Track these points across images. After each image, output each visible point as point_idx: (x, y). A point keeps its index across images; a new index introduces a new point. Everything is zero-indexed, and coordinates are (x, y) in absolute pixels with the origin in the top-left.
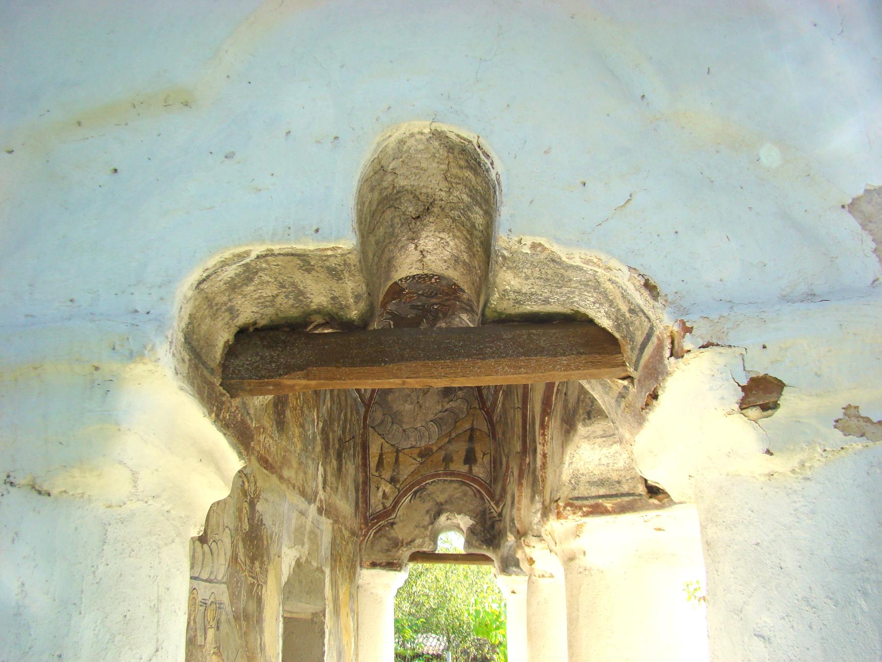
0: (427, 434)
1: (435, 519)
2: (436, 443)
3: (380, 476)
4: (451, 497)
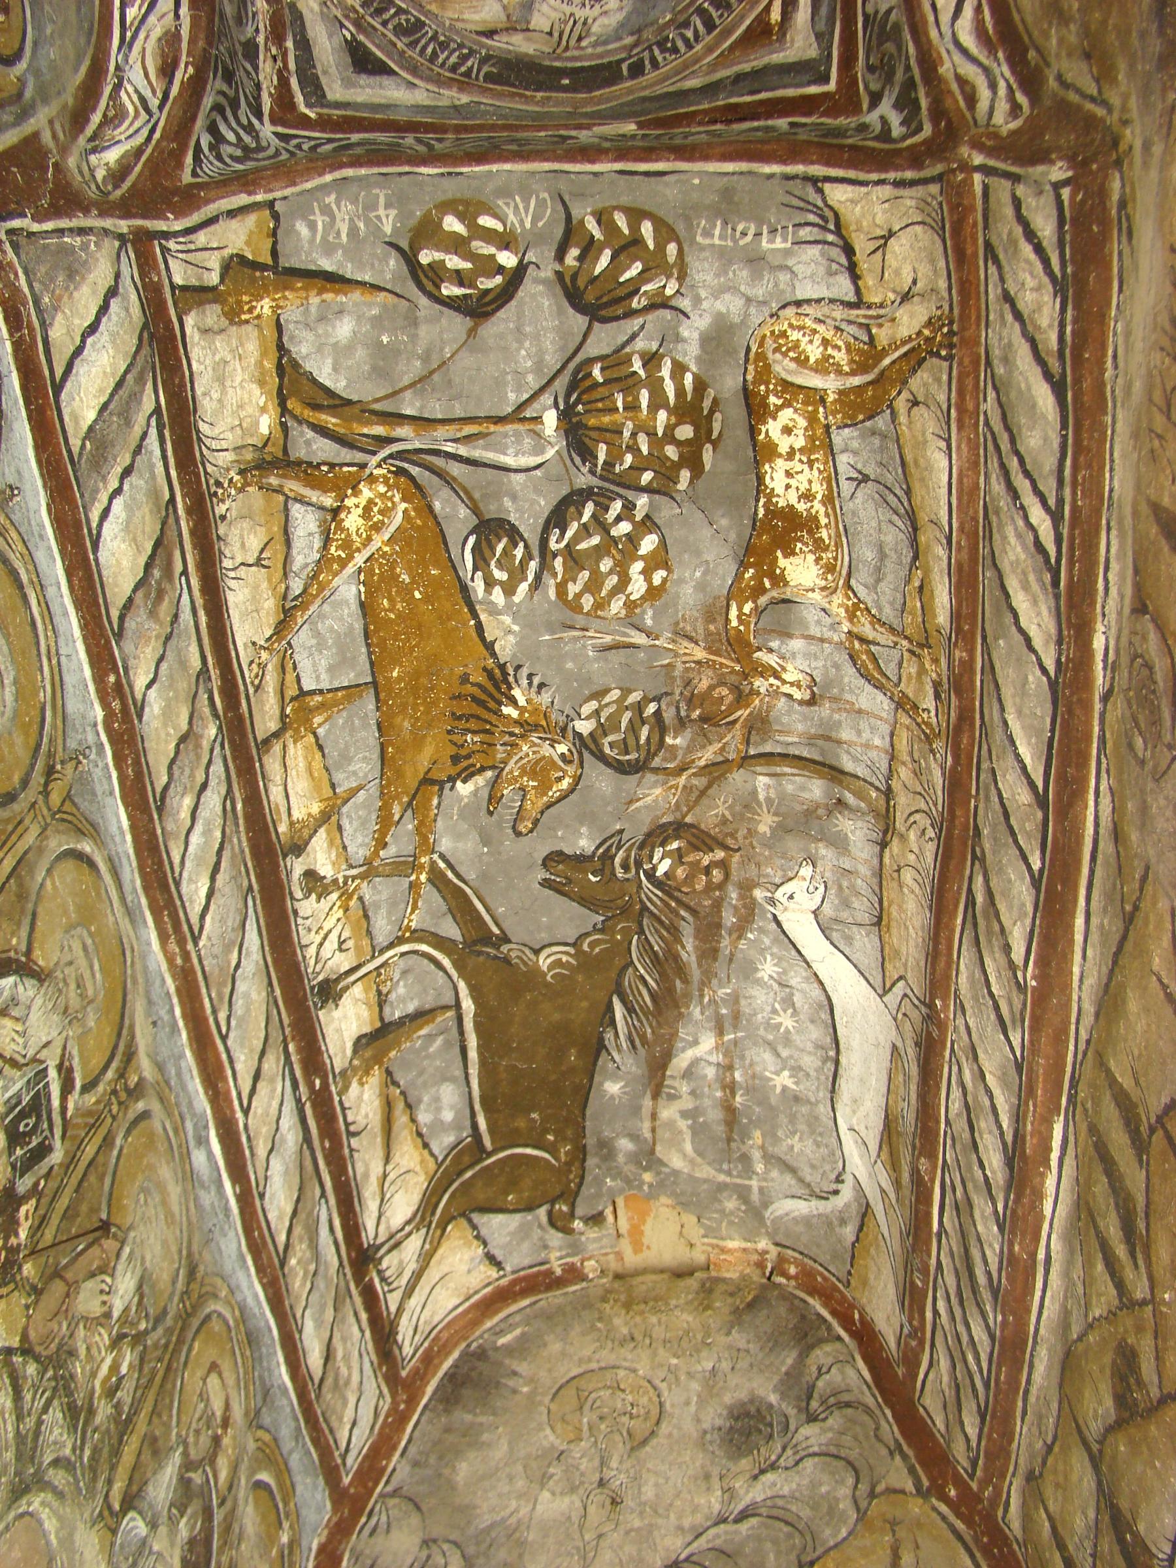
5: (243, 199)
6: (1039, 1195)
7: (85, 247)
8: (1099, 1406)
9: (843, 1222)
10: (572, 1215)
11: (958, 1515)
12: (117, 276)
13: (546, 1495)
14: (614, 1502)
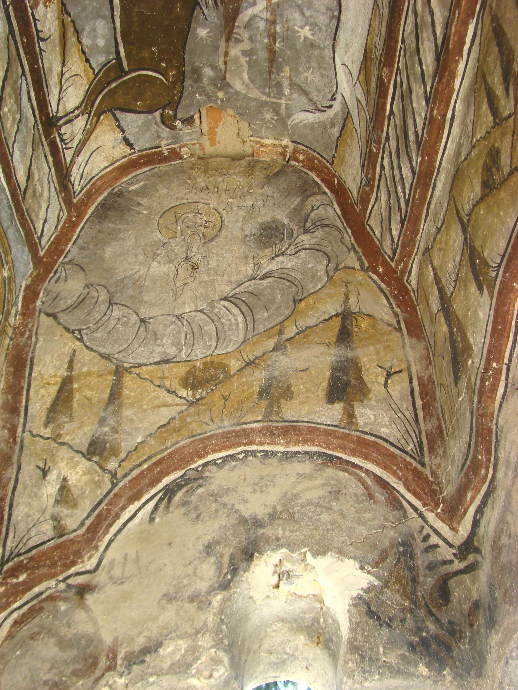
0: (210, 328)
1: (234, 571)
2: (239, 350)
3: (56, 438)
4: (288, 499)
6: (453, 76)
8: (472, 190)
9: (333, 125)
10: (175, 117)
11: (383, 281)
13: (155, 264)
14: (193, 268)
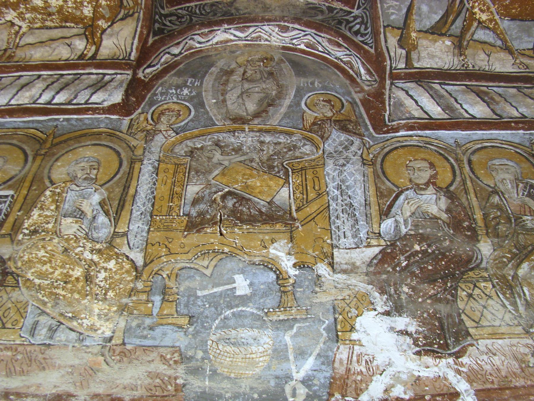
5: (382, 36)
7: (394, 98)
12: (402, 89)
